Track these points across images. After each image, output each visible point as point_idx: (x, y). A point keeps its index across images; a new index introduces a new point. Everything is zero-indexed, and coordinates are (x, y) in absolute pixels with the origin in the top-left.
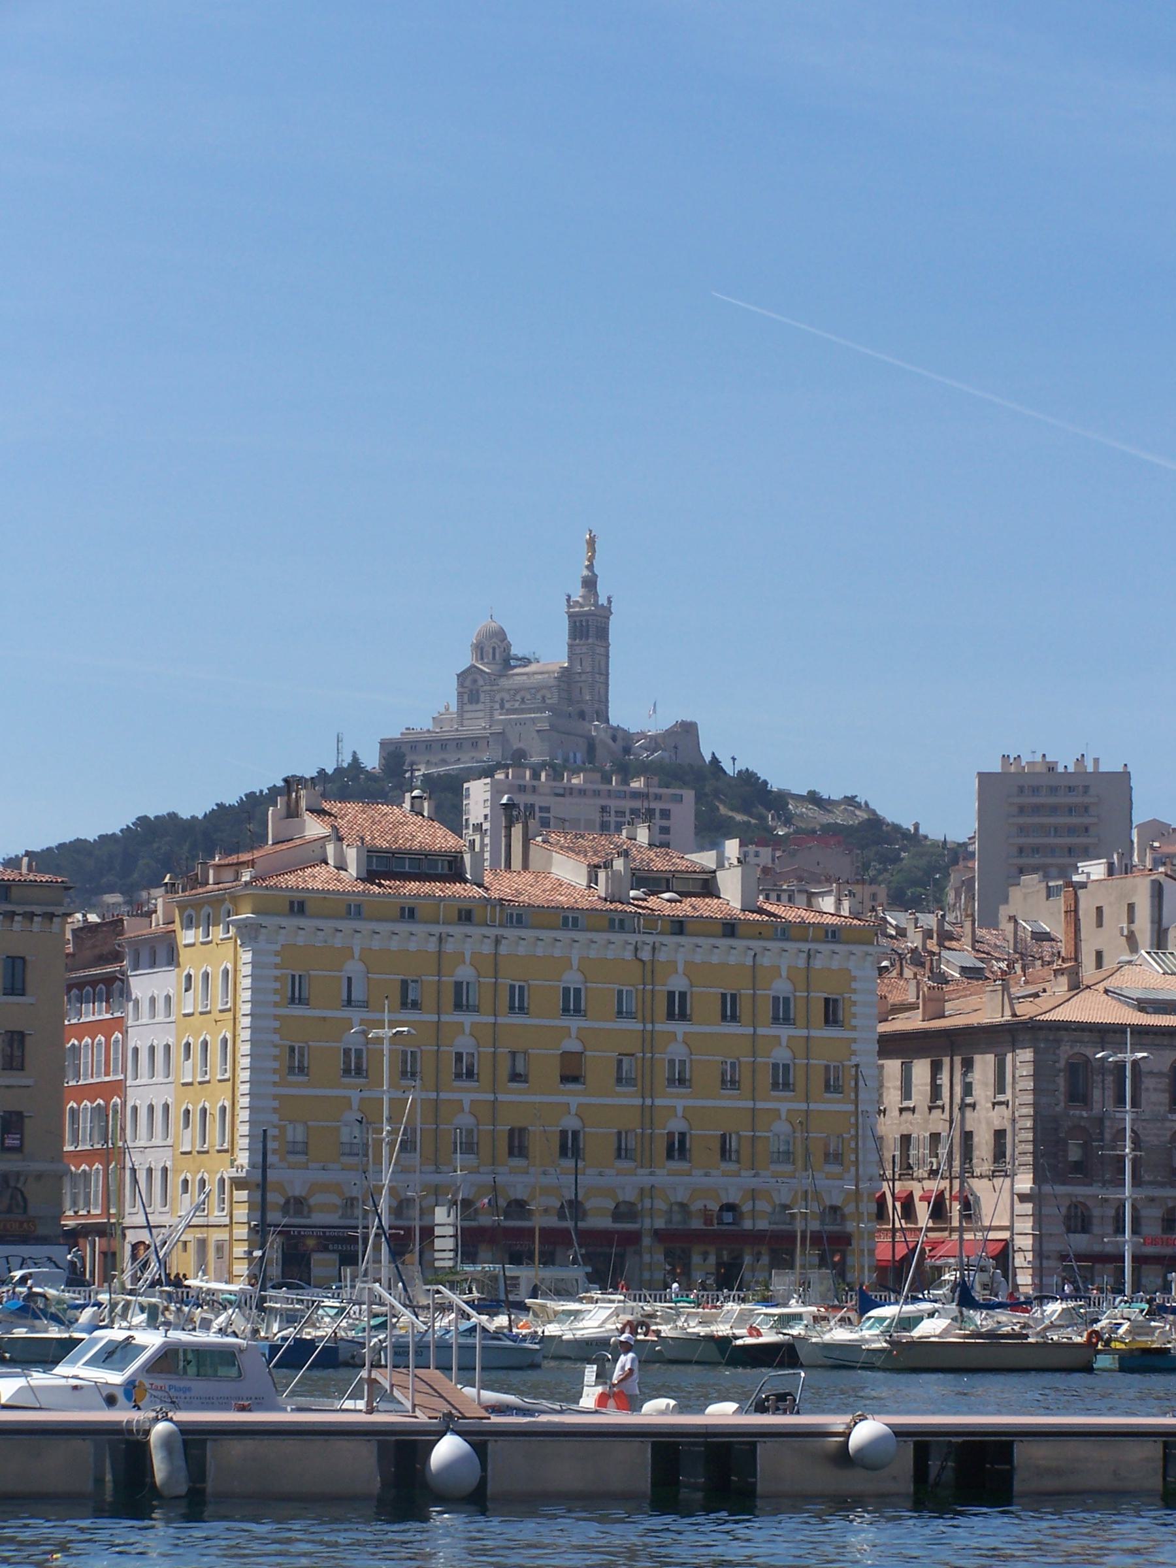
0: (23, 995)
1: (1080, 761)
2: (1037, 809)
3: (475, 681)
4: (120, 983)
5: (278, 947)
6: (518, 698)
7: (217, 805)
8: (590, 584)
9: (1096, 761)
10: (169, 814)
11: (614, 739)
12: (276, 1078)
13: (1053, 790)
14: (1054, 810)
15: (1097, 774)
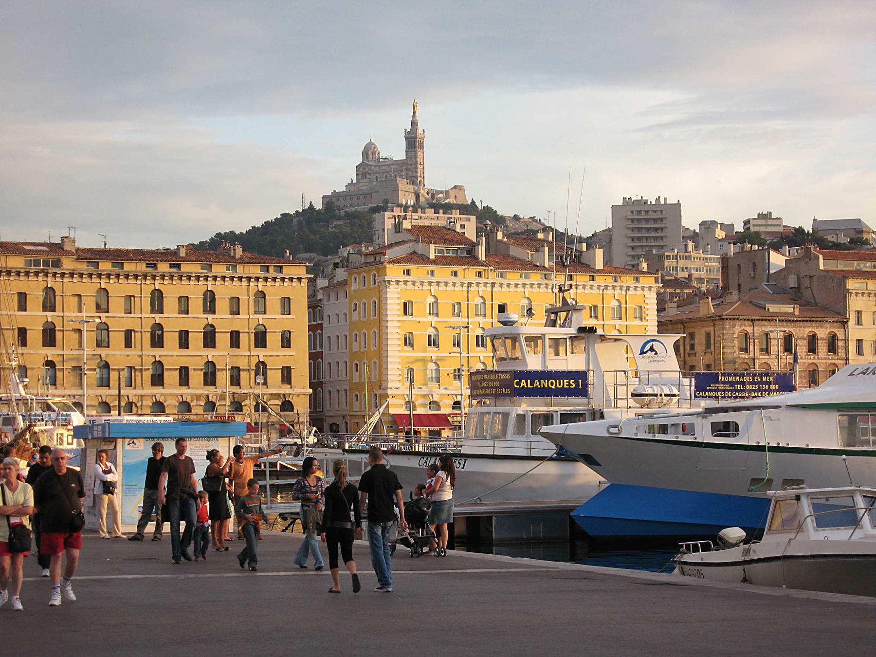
0: (289, 314)
1: (658, 200)
2: (639, 220)
3: (364, 169)
4: (320, 309)
5: (399, 290)
6: (384, 176)
7: (252, 227)
8: (414, 123)
9: (665, 199)
10: (230, 232)
11: (428, 193)
12: (400, 349)
13: (647, 212)
14: (647, 220)
15: (665, 204)
